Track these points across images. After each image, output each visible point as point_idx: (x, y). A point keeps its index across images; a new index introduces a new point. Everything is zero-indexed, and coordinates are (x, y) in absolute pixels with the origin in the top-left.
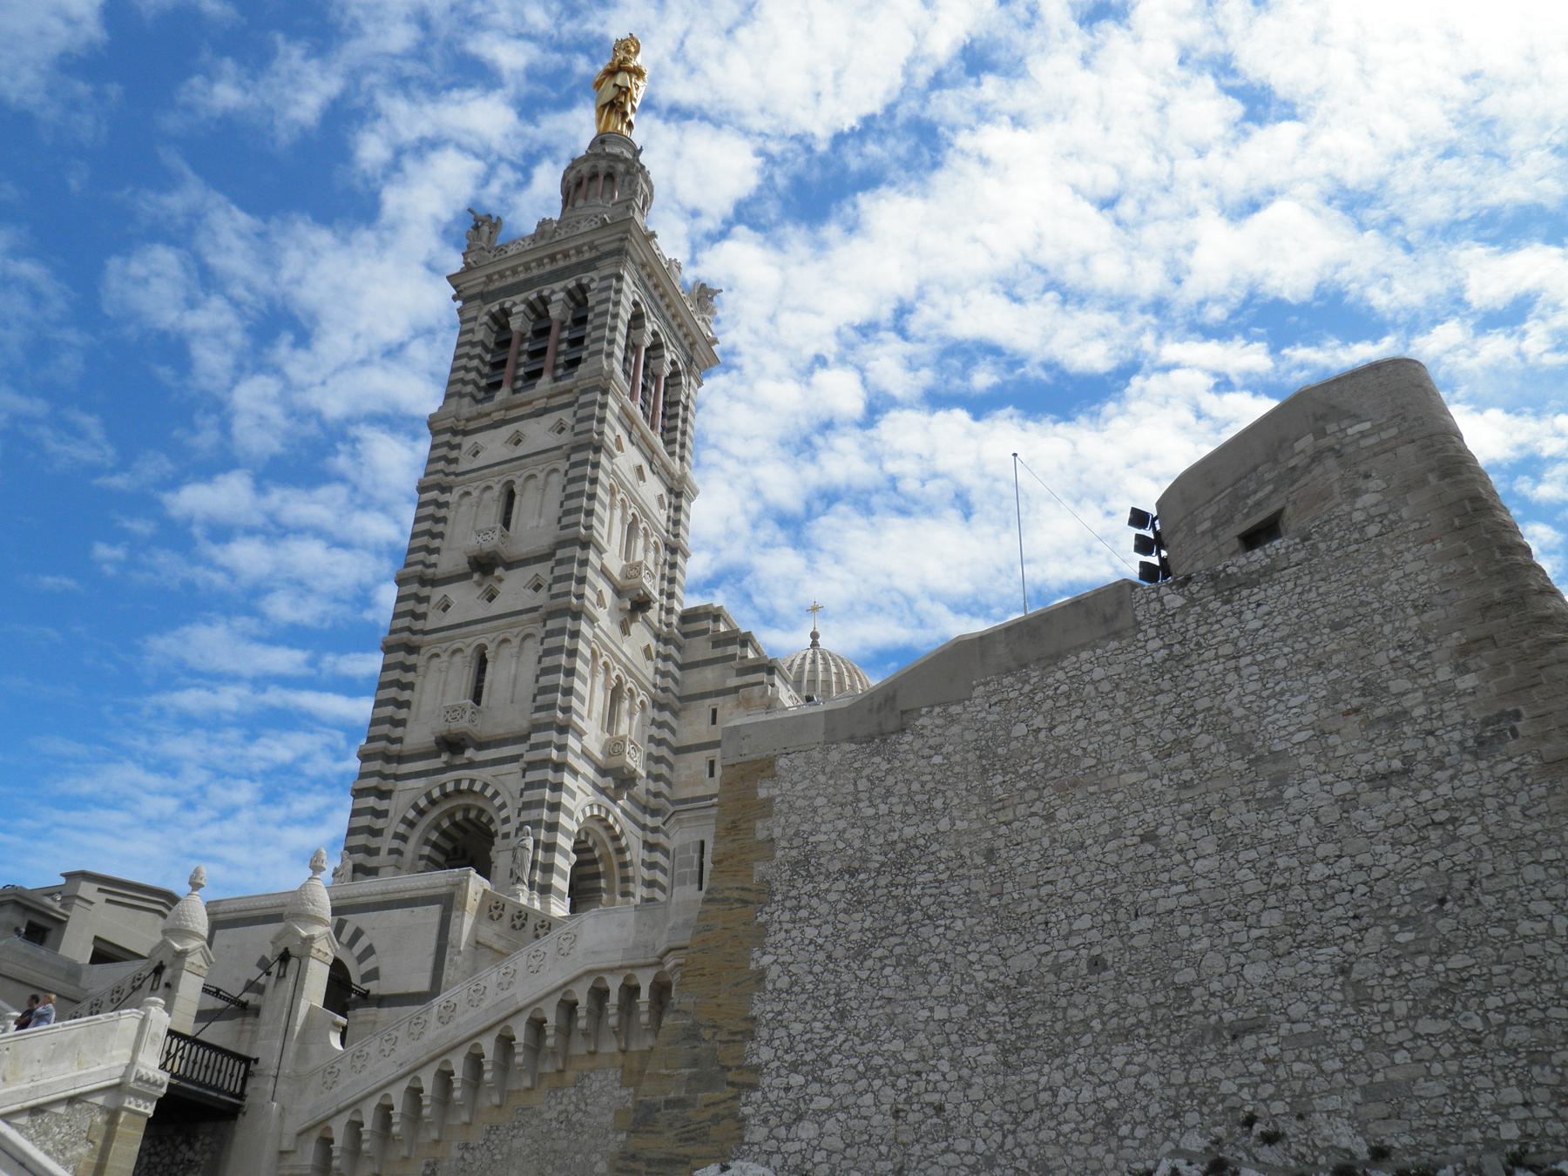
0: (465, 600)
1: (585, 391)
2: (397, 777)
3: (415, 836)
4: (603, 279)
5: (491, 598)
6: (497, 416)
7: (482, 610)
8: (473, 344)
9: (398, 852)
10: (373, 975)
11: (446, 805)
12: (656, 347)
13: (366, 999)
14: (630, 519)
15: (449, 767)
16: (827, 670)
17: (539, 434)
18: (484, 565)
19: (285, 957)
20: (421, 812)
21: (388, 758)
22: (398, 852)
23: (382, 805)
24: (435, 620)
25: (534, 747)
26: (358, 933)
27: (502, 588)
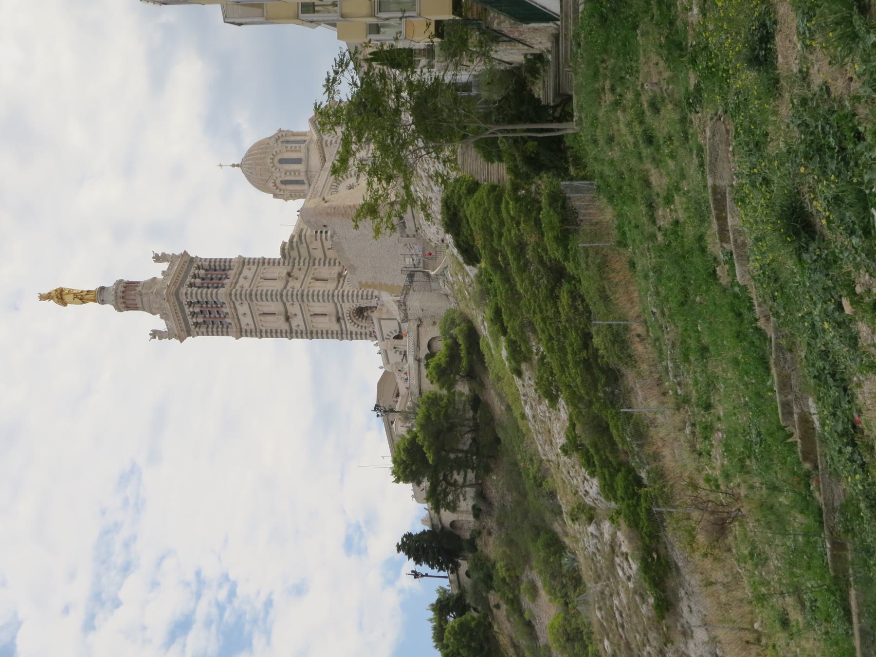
0: (296, 322)
1: (231, 299)
2: (347, 330)
3: (361, 324)
4: (187, 298)
5: (296, 315)
6: (236, 321)
7: (300, 316)
8: (207, 332)
9: (365, 327)
10: (395, 331)
11: (353, 318)
12: (195, 277)
13: (400, 332)
14: (262, 280)
15: (344, 319)
16: (249, 160)
17: (243, 309)
18: (287, 319)
19: (395, 348)
20: (355, 324)
21: (342, 333)
22: (365, 327)
23: (354, 333)
24: (302, 327)
25: (339, 301)
26: (388, 335)
27: (293, 313)
